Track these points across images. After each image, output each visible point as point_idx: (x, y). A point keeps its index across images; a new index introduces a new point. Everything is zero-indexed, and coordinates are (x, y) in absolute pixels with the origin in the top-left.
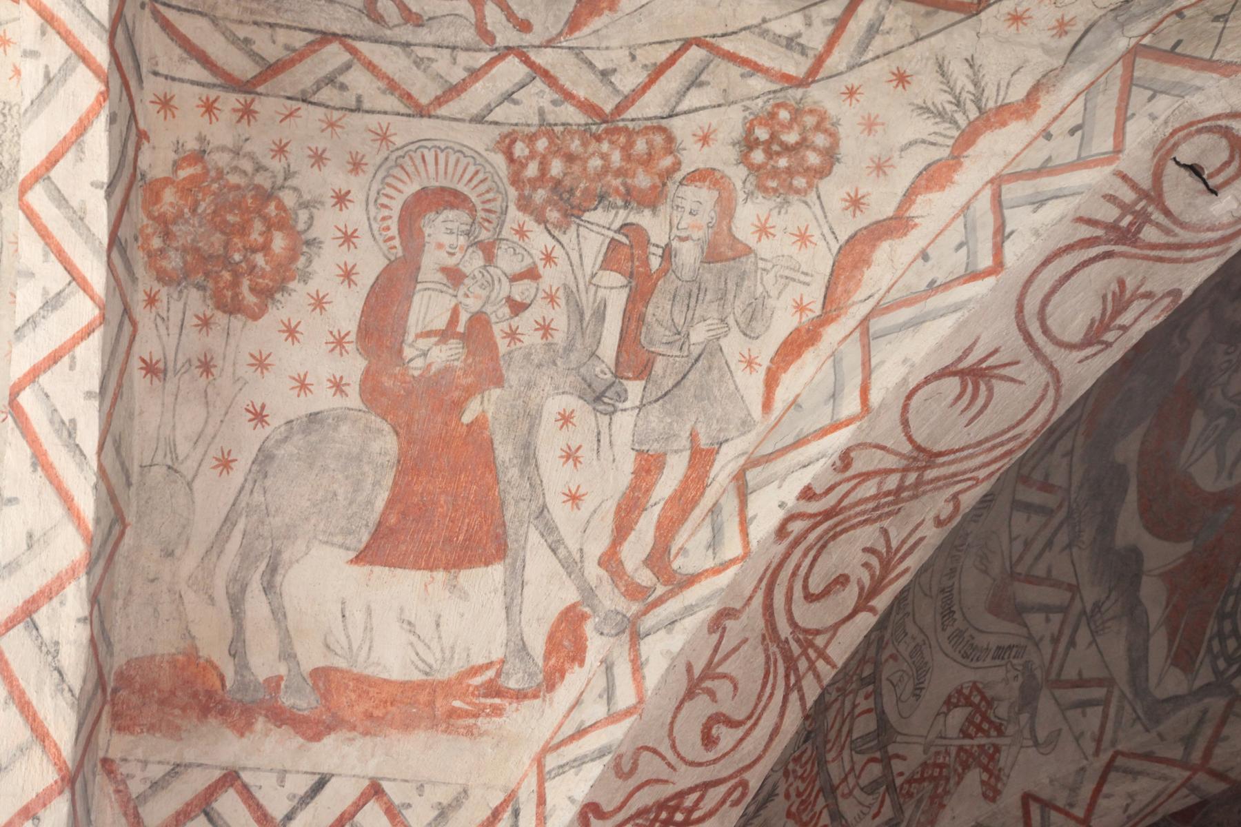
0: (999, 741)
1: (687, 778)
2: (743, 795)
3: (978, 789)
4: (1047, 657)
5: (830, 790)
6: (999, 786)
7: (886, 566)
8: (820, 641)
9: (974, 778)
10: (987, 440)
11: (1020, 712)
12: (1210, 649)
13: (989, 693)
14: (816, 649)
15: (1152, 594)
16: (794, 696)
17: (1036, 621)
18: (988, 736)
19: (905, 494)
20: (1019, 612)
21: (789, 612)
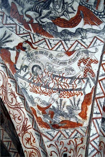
0: (90, 59)
1: (22, 124)
2: (27, 119)
3: (95, 64)
4: (84, 47)
5: (73, 90)
6: (97, 61)
7: (12, 93)
8: (17, 103)
9: (92, 65)
10: (3, 79)
12: (101, 18)
13: (82, 58)
14: (18, 104)
15: (87, 26)
16: (21, 108)
17: (77, 48)
18: (88, 60)
19: (6, 89)
20: (74, 51)
21: (12, 106)
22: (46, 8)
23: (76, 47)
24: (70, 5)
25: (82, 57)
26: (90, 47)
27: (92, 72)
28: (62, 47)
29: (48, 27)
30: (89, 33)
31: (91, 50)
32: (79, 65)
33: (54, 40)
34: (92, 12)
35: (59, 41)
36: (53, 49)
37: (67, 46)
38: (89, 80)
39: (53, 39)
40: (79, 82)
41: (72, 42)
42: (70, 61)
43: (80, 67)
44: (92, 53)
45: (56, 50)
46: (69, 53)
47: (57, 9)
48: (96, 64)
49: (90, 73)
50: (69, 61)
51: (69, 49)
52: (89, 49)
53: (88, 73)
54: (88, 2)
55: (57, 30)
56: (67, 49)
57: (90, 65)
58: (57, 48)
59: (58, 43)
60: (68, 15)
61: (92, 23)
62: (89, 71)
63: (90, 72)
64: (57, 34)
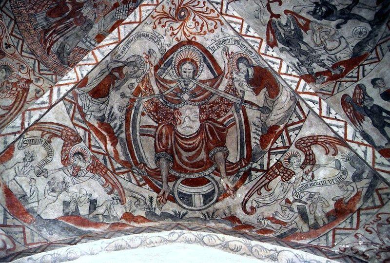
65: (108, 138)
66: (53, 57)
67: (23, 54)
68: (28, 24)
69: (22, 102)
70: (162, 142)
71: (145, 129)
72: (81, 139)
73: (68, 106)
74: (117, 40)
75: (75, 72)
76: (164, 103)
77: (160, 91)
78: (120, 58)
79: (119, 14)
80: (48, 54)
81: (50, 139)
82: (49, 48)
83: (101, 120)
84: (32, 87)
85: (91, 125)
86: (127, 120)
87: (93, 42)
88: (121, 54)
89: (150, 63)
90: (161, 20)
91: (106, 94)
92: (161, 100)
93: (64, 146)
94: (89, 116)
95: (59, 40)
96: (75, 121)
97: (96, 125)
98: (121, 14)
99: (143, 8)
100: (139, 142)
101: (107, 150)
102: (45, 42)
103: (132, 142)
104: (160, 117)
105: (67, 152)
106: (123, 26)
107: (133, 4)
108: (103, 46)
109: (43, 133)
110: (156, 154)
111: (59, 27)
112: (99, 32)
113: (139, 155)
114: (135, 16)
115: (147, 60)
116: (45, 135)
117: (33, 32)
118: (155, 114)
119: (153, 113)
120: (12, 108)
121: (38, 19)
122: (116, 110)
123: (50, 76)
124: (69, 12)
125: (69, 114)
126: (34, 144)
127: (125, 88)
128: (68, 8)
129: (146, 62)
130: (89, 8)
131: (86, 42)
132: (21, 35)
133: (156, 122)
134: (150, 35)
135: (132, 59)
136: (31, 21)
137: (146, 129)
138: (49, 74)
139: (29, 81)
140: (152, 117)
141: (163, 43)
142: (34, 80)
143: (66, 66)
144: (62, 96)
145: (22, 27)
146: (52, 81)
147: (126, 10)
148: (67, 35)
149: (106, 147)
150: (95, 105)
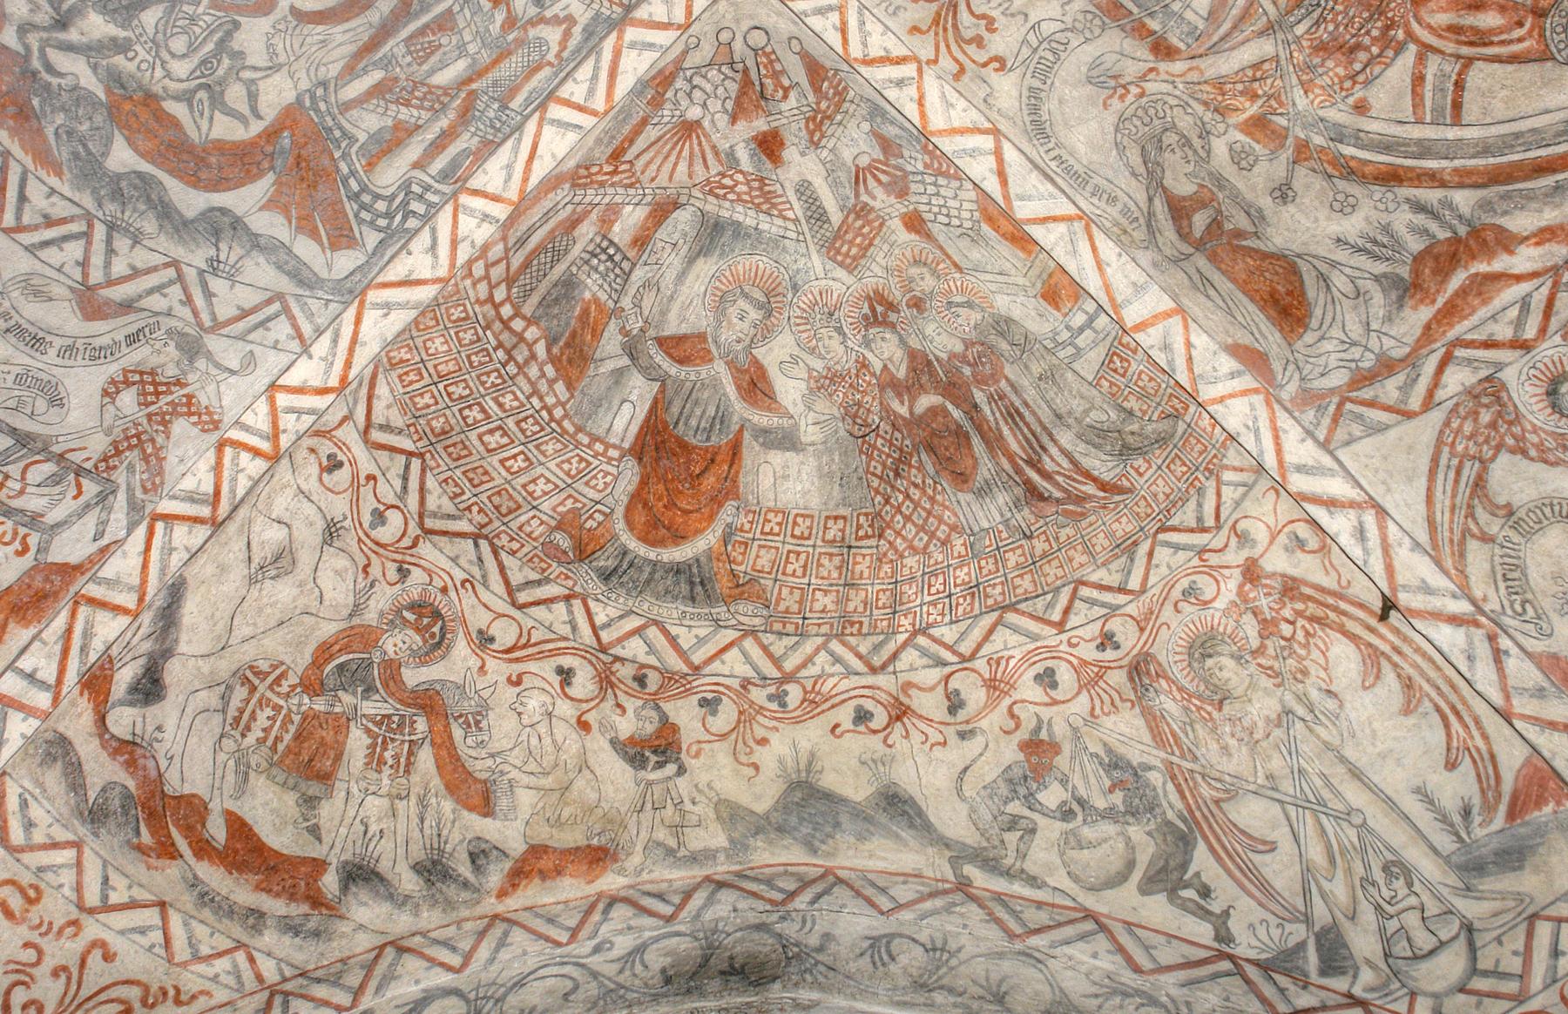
0: (185, 391)
9: (180, 426)
11: (191, 361)
12: (361, 222)
17: (156, 302)
22: (115, 11)
23: (150, 292)
24: (247, 75)
25: (154, 361)
26: (223, 331)
27: (154, 462)
28: (75, 250)
29: (63, 109)
30: (261, 260)
31: (224, 349)
32: (110, 392)
33: (53, 191)
34: (338, 170)
35: (78, 211)
36: (18, 236)
37: (108, 264)
38: (111, 498)
39: (53, 181)
40: (55, 480)
41: (142, 258)
42: (70, 348)
43: (110, 408)
44: (218, 366)
45: (30, 249)
46: (91, 304)
47: (171, 53)
48: (204, 431)
49: (140, 466)
50: (70, 342)
51: (111, 283)
52: (213, 343)
53: (132, 456)
54: (348, 115)
55: (105, 154)
56: (96, 276)
57: (170, 422)
58: (46, 244)
59: (63, 221)
60: (211, 118)
61: (304, 222)
62: (144, 451)
63: (146, 458)
64: (90, 170)
65: (1481, 267)
66: (1141, 475)
67: (1134, 583)
68: (1012, 559)
69: (1343, 605)
70: (1492, 31)
71: (1428, 103)
72: (1488, 379)
73: (1357, 430)
74: (1078, 226)
75: (1222, 400)
76: (1315, 15)
77: (1260, 34)
78: (1133, 208)
79: (954, 212)
80: (1130, 491)
81: (1498, 507)
82: (1103, 486)
83: (1407, 290)
84: (1277, 562)
85: (1423, 334)
86: (1391, 177)
87: (1079, 319)
88: (1119, 206)
89: (1143, 78)
90: (968, 34)
91: (1287, 265)
92: (1300, 30)
93: (1524, 453)
94: (1385, 339)
95: (1069, 447)
96: (1415, 403)
97: (1426, 313)
98: (951, 203)
99: (937, 121)
100: (1494, 130)
101: (1534, 275)
102: (1081, 499)
103: (1491, 160)
104: (1375, 33)
105: (1550, 443)
106: (1016, 204)
107: (906, 153)
108: (1107, 288)
109: (1473, 536)
110: (1554, 59)
111: (1014, 446)
112: (1031, 292)
113: (1559, 134)
114: (973, 153)
115: (1134, 90)
116: (1481, 530)
117: (1040, 546)
118: (1362, 56)
119: (1358, 66)
120: (1370, 645)
121: (986, 525)
122: (1353, 226)
123: (1229, 494)
124: (950, 407)
125: (1387, 427)
126: (1526, 576)
127: (1255, 184)
128: (933, 411)
129: (1142, 95)
130: (930, 329)
131: (1076, 347)
132: (1057, 590)
133: (1397, 53)
134: (1029, 81)
135: (1134, 157)
136: (998, 548)
137: (1428, 95)
138: (1219, 494)
139: (1251, 572)
140: (1377, 69)
141: (1057, 26)
142: (1245, 553)
143: (1181, 427)
144: (1327, 461)
145: (1026, 583)
146: (1249, 487)
147: (935, 184)
148: (1046, 415)
149: (1519, 278)
150: (1339, 317)
